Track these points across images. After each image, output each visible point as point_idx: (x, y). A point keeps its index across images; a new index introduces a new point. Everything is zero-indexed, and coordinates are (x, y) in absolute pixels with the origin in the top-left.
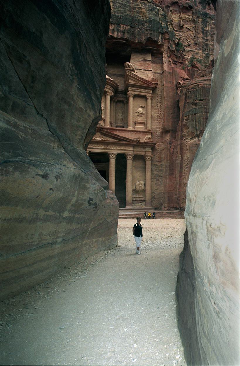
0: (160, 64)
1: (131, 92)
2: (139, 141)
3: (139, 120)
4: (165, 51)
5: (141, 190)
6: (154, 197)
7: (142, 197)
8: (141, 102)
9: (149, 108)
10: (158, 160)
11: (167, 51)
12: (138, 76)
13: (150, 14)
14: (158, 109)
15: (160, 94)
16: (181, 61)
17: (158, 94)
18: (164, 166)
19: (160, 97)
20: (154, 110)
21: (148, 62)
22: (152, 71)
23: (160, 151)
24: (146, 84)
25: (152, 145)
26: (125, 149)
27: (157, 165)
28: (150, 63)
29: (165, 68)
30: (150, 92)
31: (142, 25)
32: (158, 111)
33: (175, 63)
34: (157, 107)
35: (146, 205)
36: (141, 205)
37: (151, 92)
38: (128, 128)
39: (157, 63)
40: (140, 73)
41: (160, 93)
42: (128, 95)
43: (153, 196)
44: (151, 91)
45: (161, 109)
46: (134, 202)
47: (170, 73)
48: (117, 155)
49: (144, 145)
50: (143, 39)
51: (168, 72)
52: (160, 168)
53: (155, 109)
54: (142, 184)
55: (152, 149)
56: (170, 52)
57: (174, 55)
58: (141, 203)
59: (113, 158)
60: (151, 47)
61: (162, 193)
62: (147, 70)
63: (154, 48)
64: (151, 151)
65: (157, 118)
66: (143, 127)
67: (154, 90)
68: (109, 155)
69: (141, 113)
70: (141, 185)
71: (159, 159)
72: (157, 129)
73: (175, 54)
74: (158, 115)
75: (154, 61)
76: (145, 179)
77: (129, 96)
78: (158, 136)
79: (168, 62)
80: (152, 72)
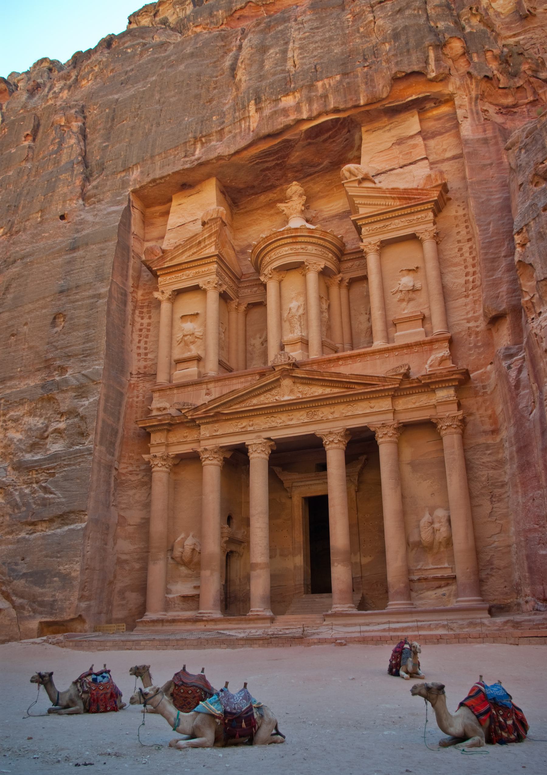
0: (453, 131)
1: (370, 241)
2: (406, 375)
3: (406, 312)
4: (459, 88)
5: (440, 543)
6: (490, 562)
7: (446, 565)
10: (488, 427)
11: (468, 87)
12: (379, 188)
13: (394, 21)
14: (465, 260)
15: (464, 215)
16: (531, 99)
17: (456, 217)
18: (507, 445)
19: (466, 221)
20: (450, 269)
21: (412, 142)
22: (426, 158)
23: (492, 393)
24: (410, 199)
25: (454, 377)
26: (368, 411)
27: (488, 447)
28: (419, 140)
29: (466, 133)
31: (373, 57)
32: (466, 267)
33: (507, 110)
34: (462, 255)
35: (457, 595)
36: (444, 595)
37: (431, 215)
38: (371, 343)
39: (441, 134)
41: (464, 212)
43: (488, 558)
45: (474, 258)
46: (416, 585)
47: (485, 141)
48: (342, 434)
49: (428, 385)
50: (381, 87)
51: (478, 140)
52: (500, 456)
53: (456, 265)
54: (440, 522)
55: (456, 391)
56: (477, 86)
57: (500, 88)
58: (440, 587)
59: (334, 445)
60: (412, 96)
61: (515, 545)
62: (411, 164)
63: (420, 96)
64: (455, 398)
66: (422, 329)
67: (438, 208)
68: (321, 440)
70: (436, 526)
71: (491, 425)
72: (471, 324)
73: (501, 86)
75: (432, 133)
76: (448, 502)
78: (475, 345)
79: (477, 113)
80: (426, 161)
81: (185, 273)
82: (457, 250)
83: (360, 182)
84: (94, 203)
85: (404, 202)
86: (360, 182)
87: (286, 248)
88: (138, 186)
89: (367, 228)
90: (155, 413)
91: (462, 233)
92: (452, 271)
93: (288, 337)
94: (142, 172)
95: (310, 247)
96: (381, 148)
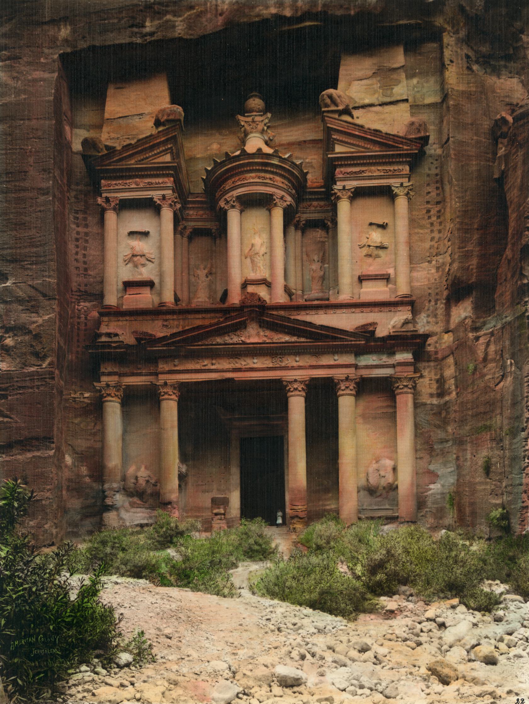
1: (344, 184)
3: (371, 268)
5: (384, 488)
7: (387, 507)
8: (375, 210)
9: (402, 225)
15: (437, 175)
19: (437, 182)
20: (416, 231)
22: (407, 100)
30: (404, 172)
32: (432, 231)
40: (370, 115)
41: (438, 171)
42: (335, 194)
44: (407, 168)
45: (441, 223)
51: (463, 92)
53: (422, 227)
65: (428, 254)
69: (377, 247)
70: (382, 473)
74: (433, 243)
77: (338, 198)
81: (134, 180)
82: (425, 211)
83: (341, 113)
84: (9, 58)
85: (384, 149)
86: (341, 113)
87: (253, 175)
88: (69, 50)
89: (342, 169)
90: (104, 339)
91: (432, 194)
92: (418, 233)
93: (252, 276)
94: (74, 31)
95: (278, 178)
96: (360, 74)
